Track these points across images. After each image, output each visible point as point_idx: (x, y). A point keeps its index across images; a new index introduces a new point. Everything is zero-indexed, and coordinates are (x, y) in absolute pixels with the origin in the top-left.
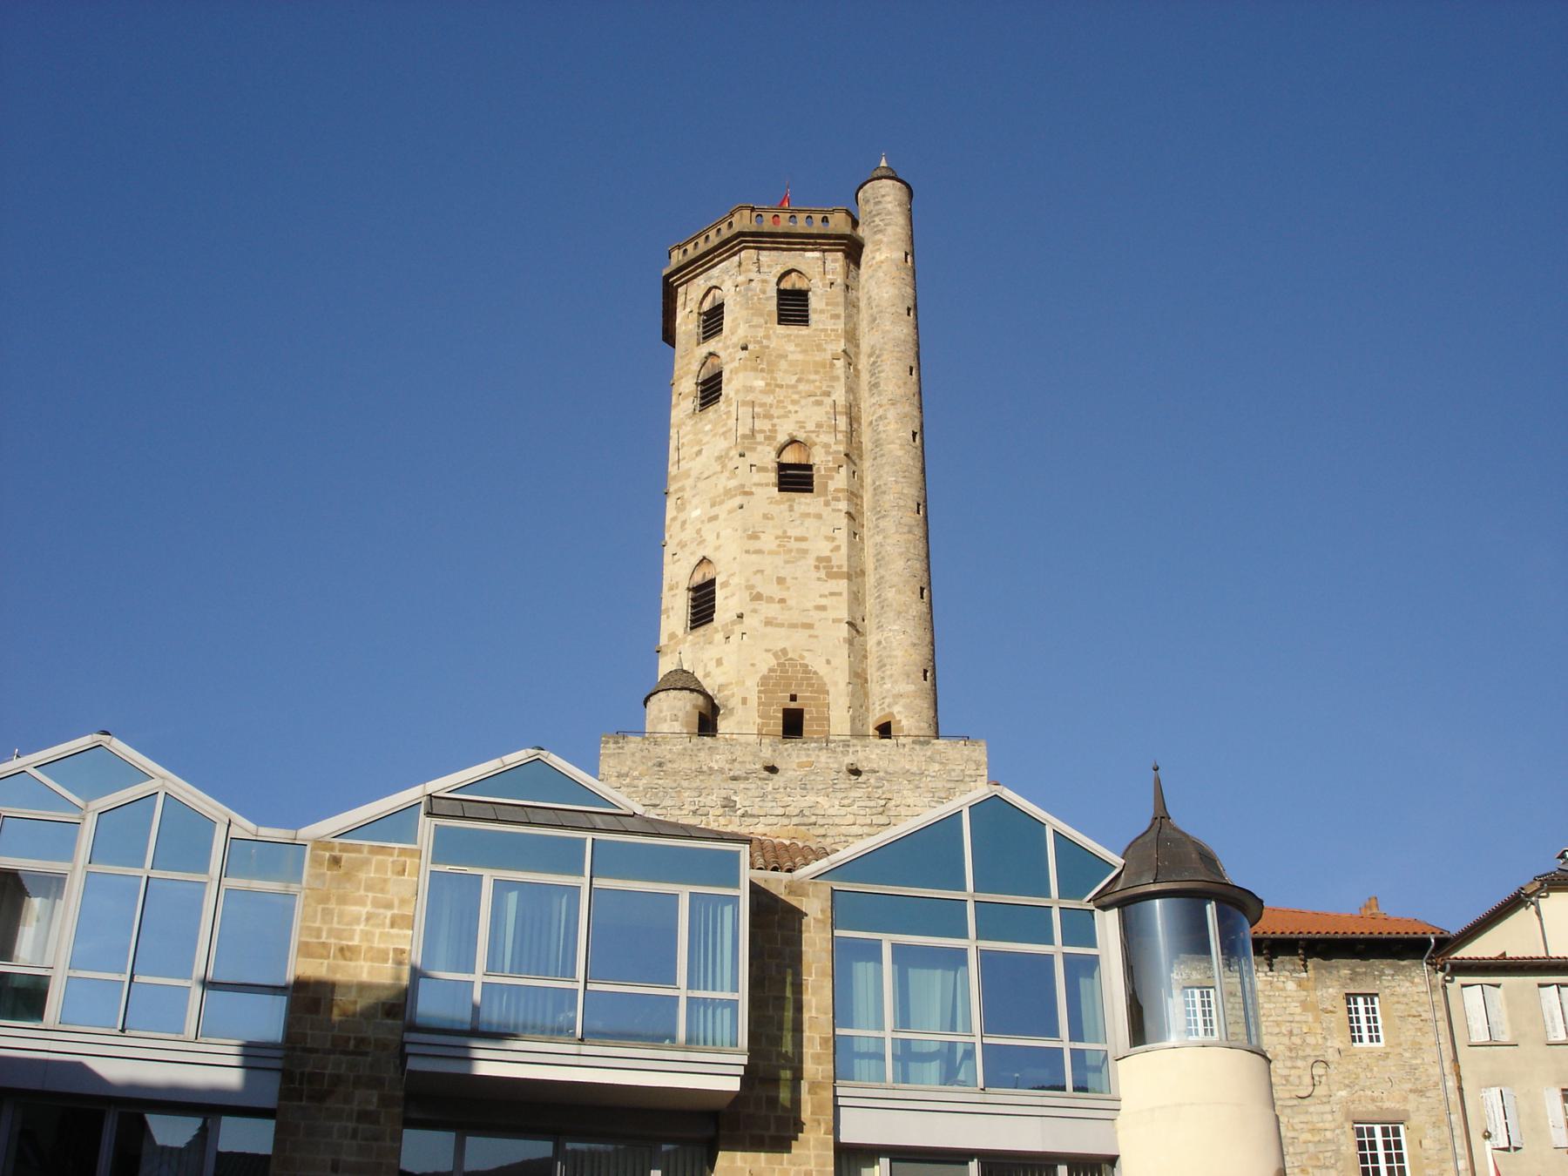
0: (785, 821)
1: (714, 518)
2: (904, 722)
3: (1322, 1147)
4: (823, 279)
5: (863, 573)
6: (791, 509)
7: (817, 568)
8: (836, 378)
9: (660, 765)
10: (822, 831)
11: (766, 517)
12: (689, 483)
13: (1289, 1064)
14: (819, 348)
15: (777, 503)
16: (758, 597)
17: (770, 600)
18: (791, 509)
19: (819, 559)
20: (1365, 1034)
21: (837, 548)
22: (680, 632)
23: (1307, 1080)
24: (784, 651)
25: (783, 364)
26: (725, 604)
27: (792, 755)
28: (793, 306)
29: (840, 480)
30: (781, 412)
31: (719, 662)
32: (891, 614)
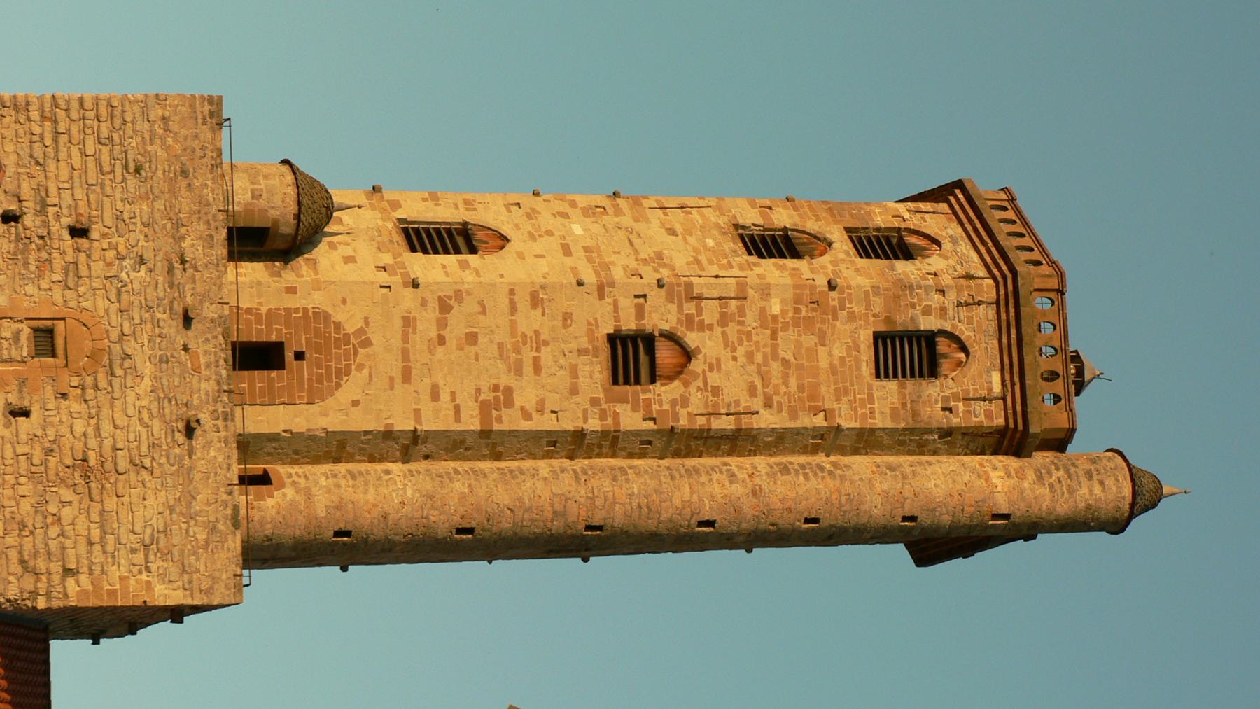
1: (567, 250)
2: (270, 502)
4: (956, 397)
5: (498, 457)
6: (582, 352)
7: (496, 388)
9: (184, 173)
10: (103, 383)
11: (567, 317)
12: (627, 220)
14: (840, 393)
15: (591, 334)
16: (445, 307)
18: (582, 352)
19: (509, 391)
21: (527, 416)
22: (400, 214)
24: (367, 343)
25: (809, 341)
26: (436, 269)
27: (211, 350)
28: (909, 352)
29: (631, 420)
30: (733, 337)
31: (349, 260)
32: (429, 486)
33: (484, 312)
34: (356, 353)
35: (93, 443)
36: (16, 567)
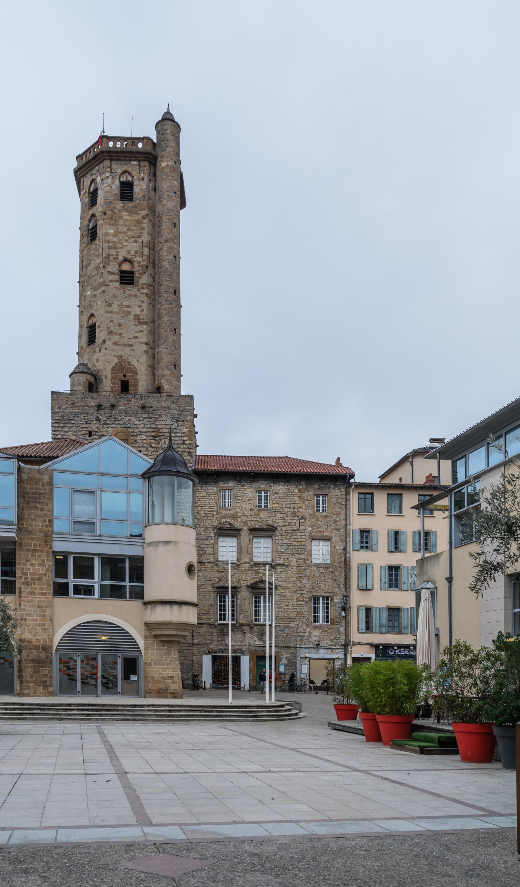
0: (119, 426)
2: (165, 387)
3: (300, 547)
6: (124, 292)
8: (143, 229)
10: (132, 430)
13: (292, 518)
15: (119, 290)
16: (111, 333)
18: (124, 292)
19: (135, 316)
20: (321, 509)
21: (142, 311)
23: (297, 524)
24: (121, 356)
25: (121, 222)
28: (126, 191)
29: (145, 279)
33: (112, 321)
34: (124, 360)
35: (149, 434)
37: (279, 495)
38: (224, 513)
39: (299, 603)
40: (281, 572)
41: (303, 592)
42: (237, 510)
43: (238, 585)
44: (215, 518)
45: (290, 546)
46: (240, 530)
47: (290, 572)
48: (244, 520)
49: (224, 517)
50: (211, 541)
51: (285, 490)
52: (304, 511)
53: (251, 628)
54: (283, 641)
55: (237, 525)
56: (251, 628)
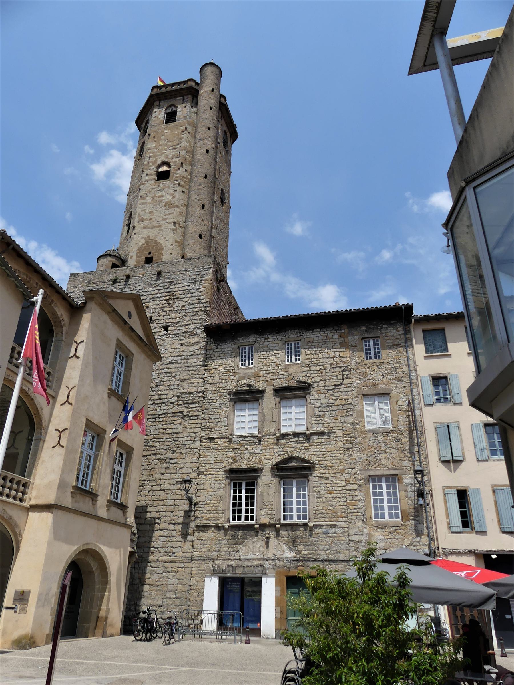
3: (345, 407)
10: (145, 297)
13: (332, 370)
16: (142, 219)
17: (146, 220)
21: (174, 197)
23: (340, 377)
24: (149, 237)
28: (171, 117)
35: (162, 299)
36: (197, 317)
37: (314, 344)
38: (242, 372)
39: (348, 487)
40: (320, 443)
41: (354, 471)
42: (259, 368)
43: (259, 466)
44: (231, 380)
45: (331, 406)
46: (262, 392)
47: (333, 443)
48: (268, 379)
49: (243, 378)
50: (225, 409)
51: (321, 338)
52: (348, 359)
53: (277, 531)
54: (327, 550)
55: (258, 385)
56: (277, 531)
